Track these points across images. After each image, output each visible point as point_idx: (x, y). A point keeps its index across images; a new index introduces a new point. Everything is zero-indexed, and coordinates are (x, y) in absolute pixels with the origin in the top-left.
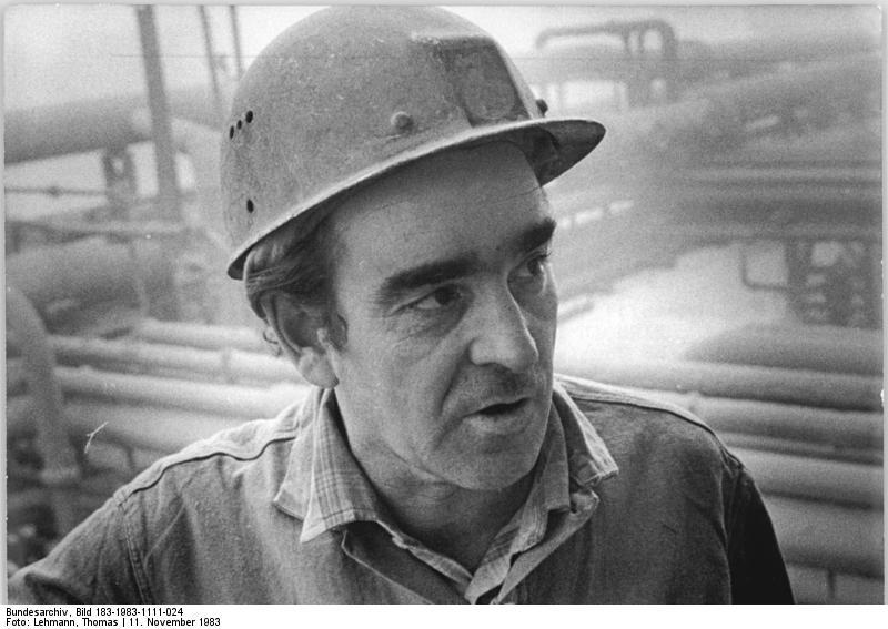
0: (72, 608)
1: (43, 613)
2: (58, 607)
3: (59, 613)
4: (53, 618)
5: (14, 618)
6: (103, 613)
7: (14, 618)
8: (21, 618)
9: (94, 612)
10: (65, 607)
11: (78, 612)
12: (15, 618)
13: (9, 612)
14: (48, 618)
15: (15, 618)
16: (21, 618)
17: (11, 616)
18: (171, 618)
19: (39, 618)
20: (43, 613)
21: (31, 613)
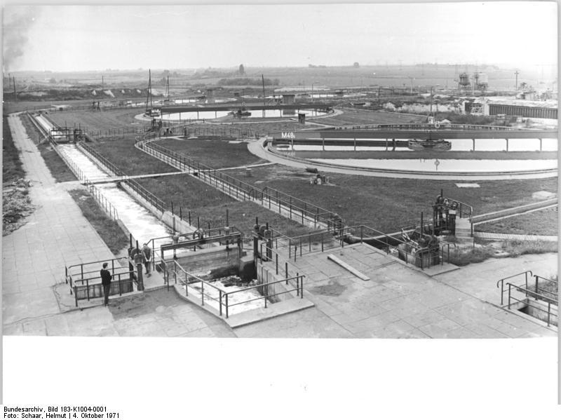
1: (27, 410)
3: (38, 410)
4: (35, 413)
5: (9, 413)
7: (9, 413)
8: (13, 413)
9: (59, 409)
11: (50, 409)
12: (10, 413)
13: (5, 409)
14: (31, 413)
15: (10, 413)
16: (13, 413)
17: (7, 412)
19: (27, 413)
20: (27, 410)
21: (20, 410)
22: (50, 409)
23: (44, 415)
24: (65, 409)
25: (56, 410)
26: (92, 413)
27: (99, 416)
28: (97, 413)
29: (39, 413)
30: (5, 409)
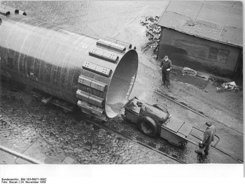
1: (12, 180)
3: (16, 180)
4: (16, 181)
6: (29, 180)
8: (6, 181)
9: (26, 179)
11: (22, 179)
12: (4, 181)
13: (2, 179)
14: (13, 181)
15: (4, 181)
16: (6, 181)
18: (32, 181)
19: (12, 181)
20: (12, 180)
21: (9, 179)
22: (22, 179)
23: (24, 181)
24: (28, 179)
25: (25, 179)
26: (31, 181)
27: (37, 182)
28: (36, 181)
29: (17, 181)
30: (2, 179)
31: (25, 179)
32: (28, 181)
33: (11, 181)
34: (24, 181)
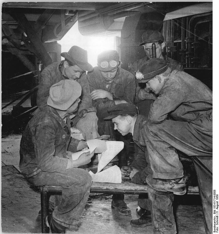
0: (214, 215)
1: (215, 223)
2: (213, 219)
3: (215, 218)
4: (216, 220)
5: (216, 230)
7: (216, 230)
8: (216, 228)
10: (213, 217)
12: (216, 230)
14: (216, 221)
15: (216, 230)
16: (216, 228)
19: (216, 223)
20: (215, 223)
21: (215, 226)
28: (216, 204)
31: (215, 210)
32: (216, 207)
33: (216, 224)
34: (217, 210)
